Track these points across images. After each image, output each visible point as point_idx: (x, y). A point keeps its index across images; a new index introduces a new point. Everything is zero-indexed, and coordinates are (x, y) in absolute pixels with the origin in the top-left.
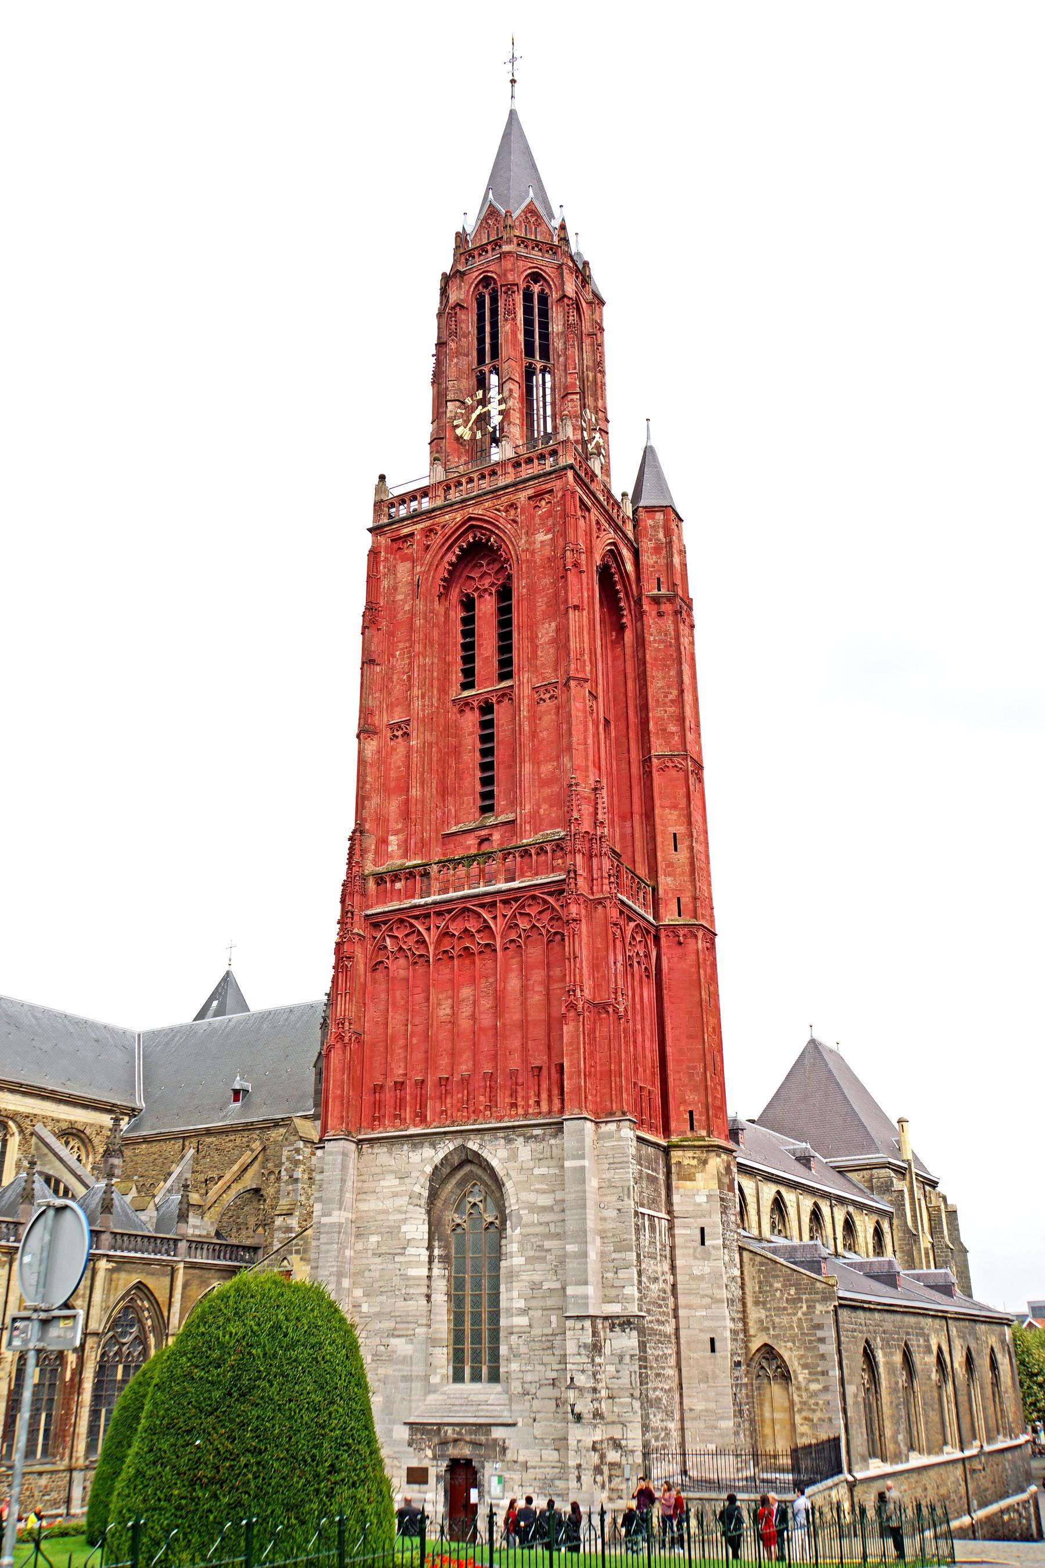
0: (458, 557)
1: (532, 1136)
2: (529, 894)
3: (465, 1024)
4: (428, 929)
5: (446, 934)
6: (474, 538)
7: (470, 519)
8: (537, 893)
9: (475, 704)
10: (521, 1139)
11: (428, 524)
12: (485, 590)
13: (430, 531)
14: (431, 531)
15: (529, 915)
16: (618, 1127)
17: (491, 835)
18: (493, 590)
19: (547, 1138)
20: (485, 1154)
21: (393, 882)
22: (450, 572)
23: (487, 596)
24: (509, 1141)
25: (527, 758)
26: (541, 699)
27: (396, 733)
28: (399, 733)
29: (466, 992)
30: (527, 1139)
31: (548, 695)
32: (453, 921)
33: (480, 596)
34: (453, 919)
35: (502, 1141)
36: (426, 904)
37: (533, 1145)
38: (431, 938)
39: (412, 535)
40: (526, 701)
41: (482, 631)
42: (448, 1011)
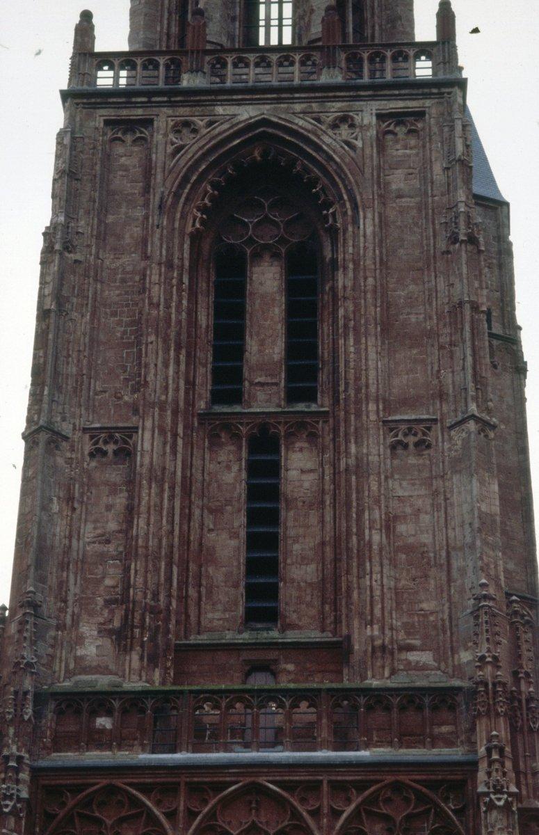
2: (390, 779)
6: (265, 154)
7: (265, 122)
9: (244, 430)
12: (266, 247)
14: (187, 124)
15: (386, 818)
17: (276, 661)
21: (94, 713)
26: (399, 442)
27: (101, 445)
28: (110, 448)
34: (226, 803)
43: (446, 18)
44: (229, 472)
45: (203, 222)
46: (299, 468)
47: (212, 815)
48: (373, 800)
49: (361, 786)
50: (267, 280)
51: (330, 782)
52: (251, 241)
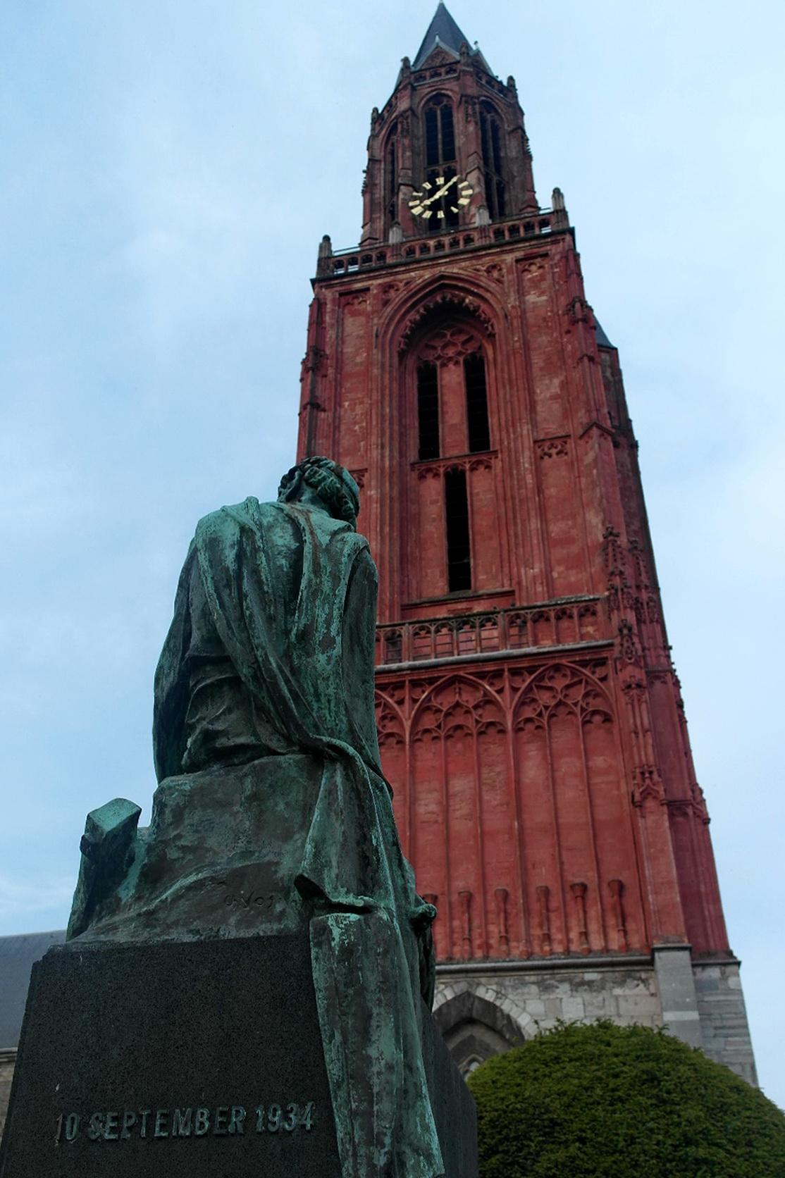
0: (422, 316)
1: (583, 983)
2: (551, 662)
3: (461, 826)
4: (400, 702)
5: (425, 708)
6: (444, 298)
7: (442, 277)
8: (564, 661)
10: (565, 987)
11: (387, 280)
12: (450, 359)
13: (387, 288)
15: (551, 689)
16: (723, 973)
18: (461, 359)
19: (609, 985)
20: (506, 1006)
22: (412, 329)
23: (451, 365)
24: (545, 988)
25: (533, 513)
29: (460, 784)
30: (577, 986)
31: (554, 451)
32: (437, 695)
33: (444, 365)
34: (439, 691)
35: (534, 989)
36: (400, 670)
37: (587, 996)
38: (406, 714)
39: (367, 289)
40: (527, 453)
41: (446, 398)
42: (433, 807)
43: (557, 194)
44: (433, 490)
45: (405, 344)
46: (480, 487)
47: (428, 699)
48: (540, 678)
49: (530, 670)
50: (452, 379)
51: (509, 670)
52: (439, 358)
